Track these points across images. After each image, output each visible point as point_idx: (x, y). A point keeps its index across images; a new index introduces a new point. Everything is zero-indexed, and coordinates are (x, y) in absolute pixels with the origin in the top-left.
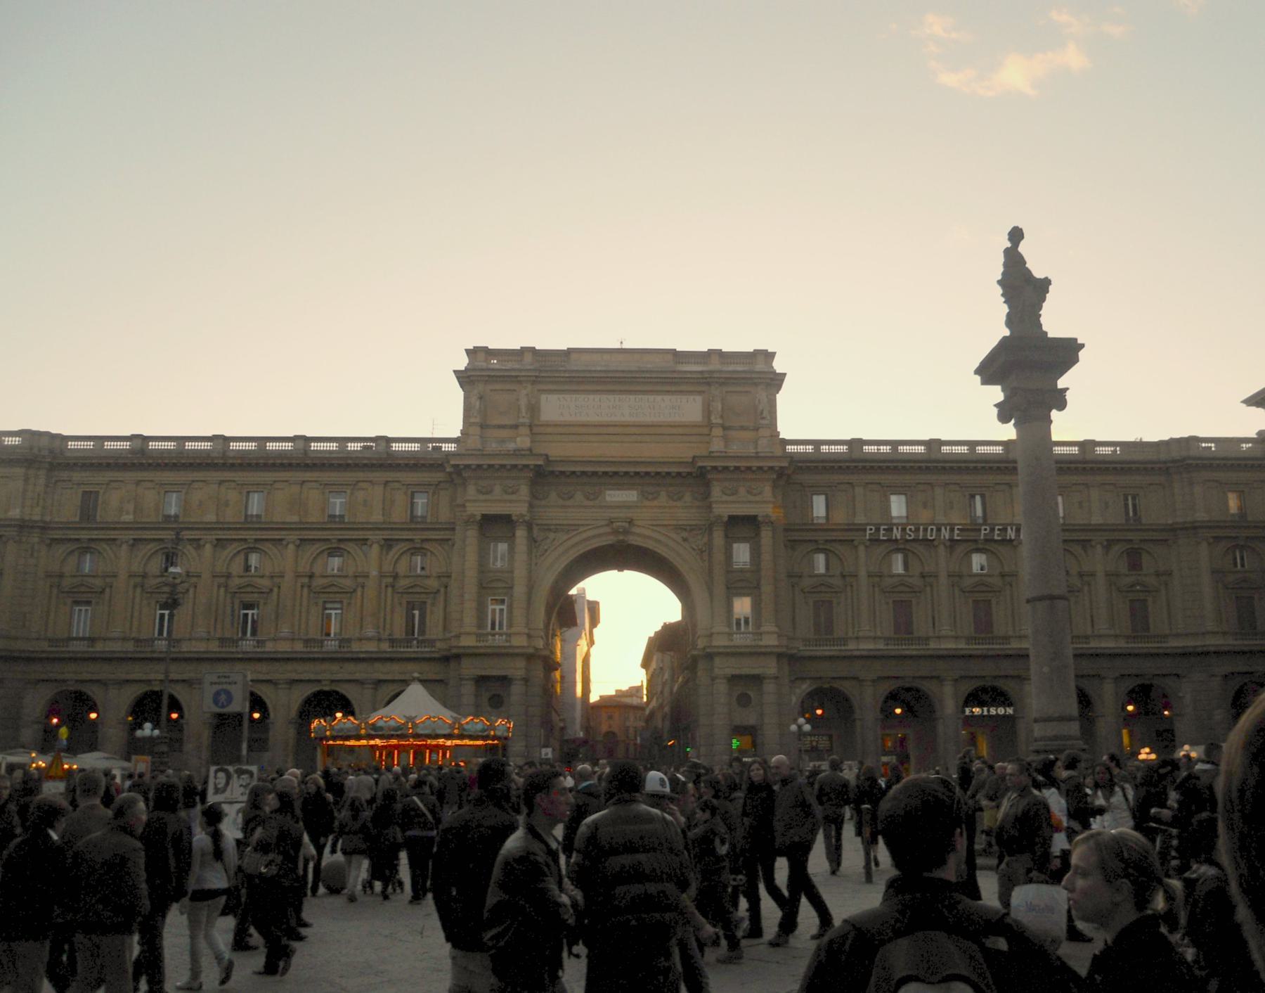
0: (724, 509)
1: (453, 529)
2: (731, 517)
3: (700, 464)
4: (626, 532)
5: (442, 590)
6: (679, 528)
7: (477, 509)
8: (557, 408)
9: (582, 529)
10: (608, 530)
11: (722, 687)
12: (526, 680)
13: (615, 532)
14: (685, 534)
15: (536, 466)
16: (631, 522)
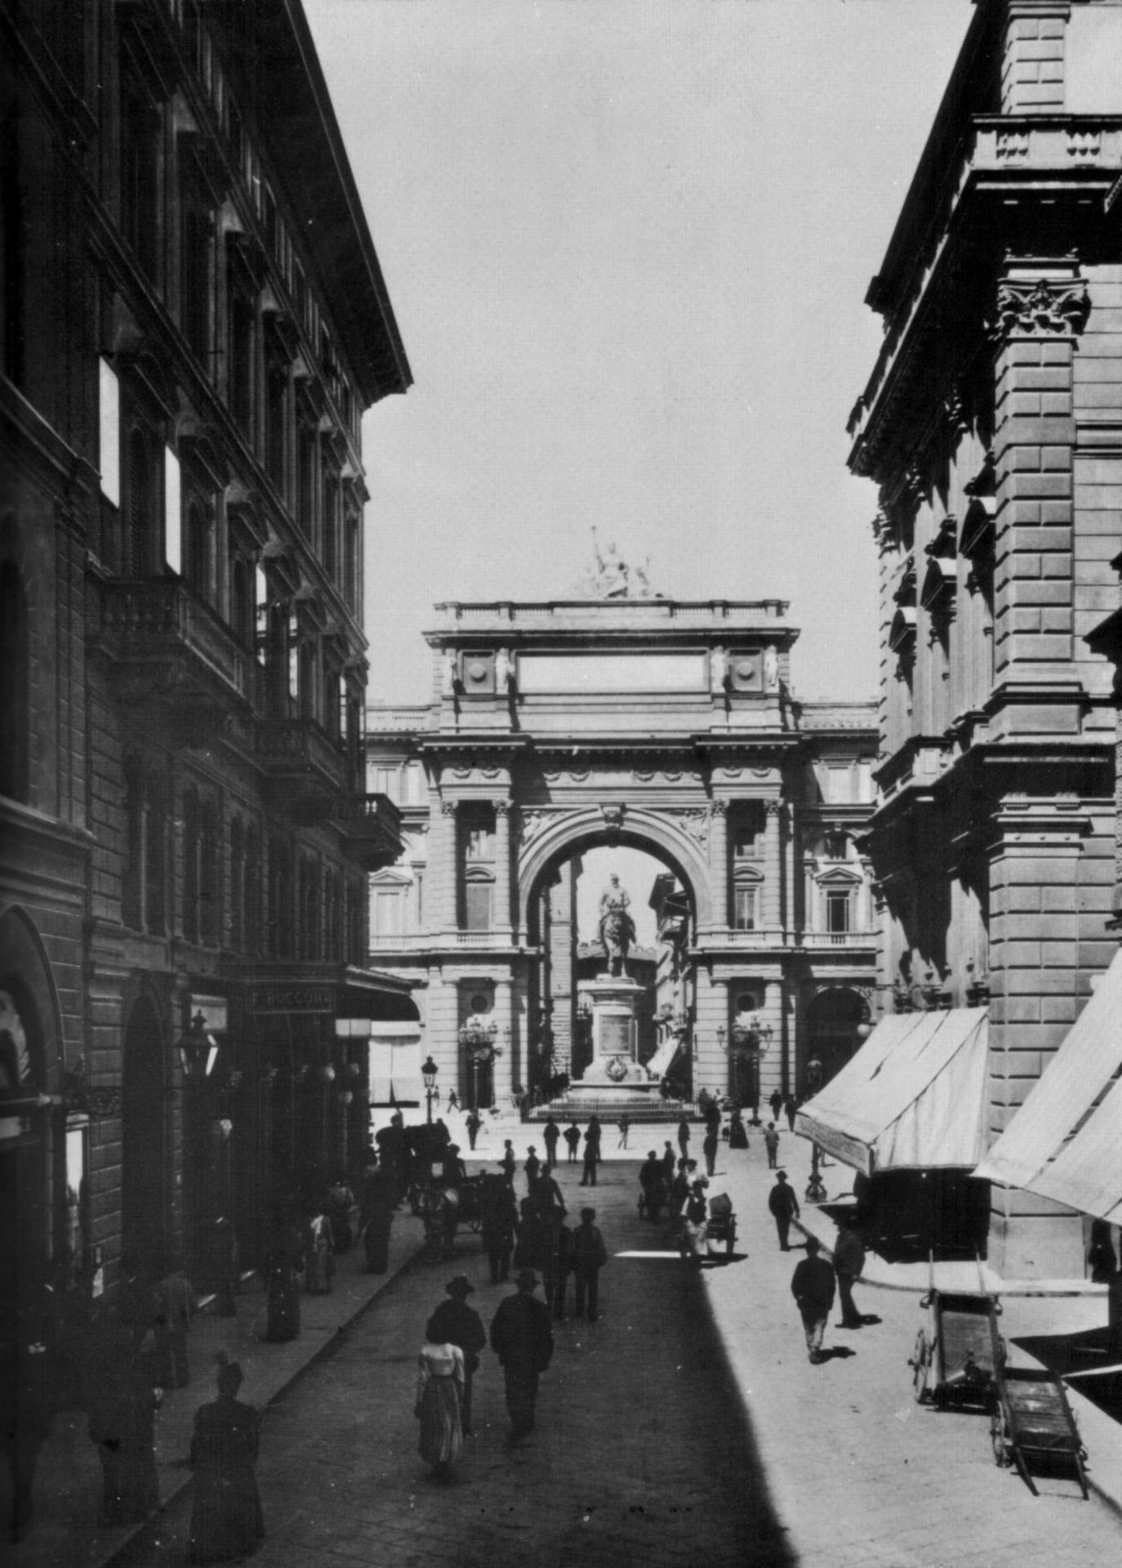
0: (724, 796)
1: (427, 814)
2: (735, 803)
3: (699, 743)
4: (619, 819)
5: (416, 881)
6: (675, 812)
7: (454, 797)
8: (540, 673)
9: (568, 814)
10: (599, 814)
11: (722, 991)
12: (512, 985)
13: (606, 818)
14: (683, 819)
15: (518, 747)
16: (624, 809)
